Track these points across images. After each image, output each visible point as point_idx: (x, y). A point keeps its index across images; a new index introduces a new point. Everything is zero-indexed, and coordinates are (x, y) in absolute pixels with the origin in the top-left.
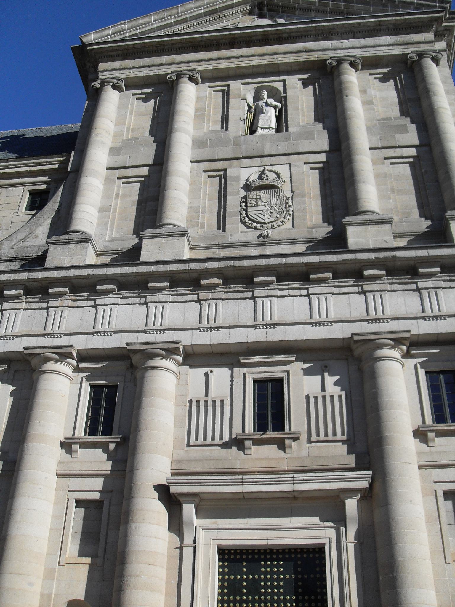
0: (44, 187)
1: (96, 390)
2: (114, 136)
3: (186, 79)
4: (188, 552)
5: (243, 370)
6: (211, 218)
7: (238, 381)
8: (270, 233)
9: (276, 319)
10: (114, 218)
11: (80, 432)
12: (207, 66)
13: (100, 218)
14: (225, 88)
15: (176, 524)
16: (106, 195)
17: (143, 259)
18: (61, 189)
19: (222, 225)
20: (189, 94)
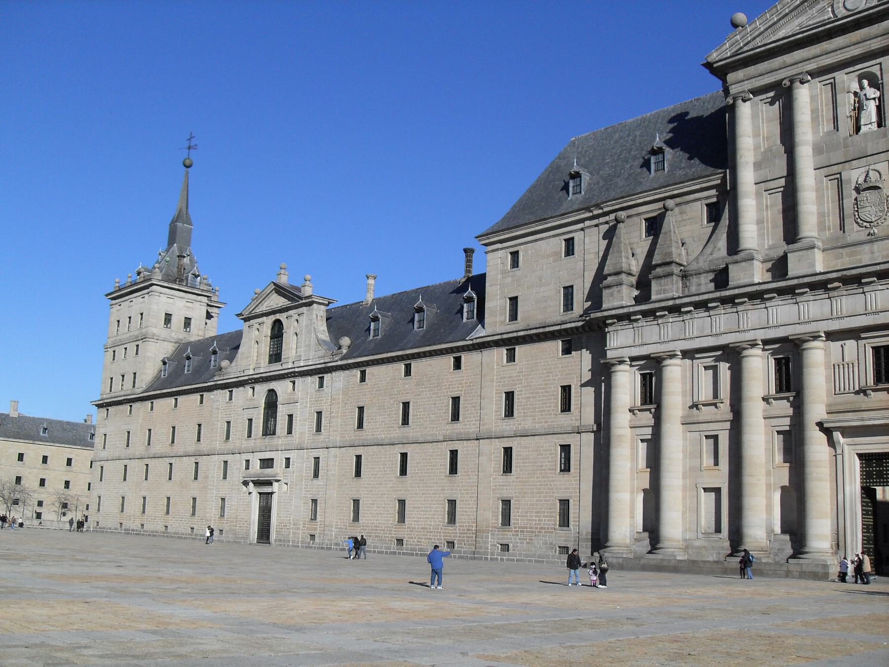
0: (714, 200)
1: (778, 362)
2: (754, 150)
3: (797, 84)
4: (839, 457)
5: (864, 341)
6: (833, 220)
7: (862, 349)
8: (876, 231)
9: (879, 308)
10: (768, 228)
11: (773, 391)
12: (812, 66)
13: (759, 230)
14: (832, 80)
15: (831, 443)
16: (759, 209)
17: (791, 274)
18: (727, 206)
19: (842, 227)
20: (803, 95)
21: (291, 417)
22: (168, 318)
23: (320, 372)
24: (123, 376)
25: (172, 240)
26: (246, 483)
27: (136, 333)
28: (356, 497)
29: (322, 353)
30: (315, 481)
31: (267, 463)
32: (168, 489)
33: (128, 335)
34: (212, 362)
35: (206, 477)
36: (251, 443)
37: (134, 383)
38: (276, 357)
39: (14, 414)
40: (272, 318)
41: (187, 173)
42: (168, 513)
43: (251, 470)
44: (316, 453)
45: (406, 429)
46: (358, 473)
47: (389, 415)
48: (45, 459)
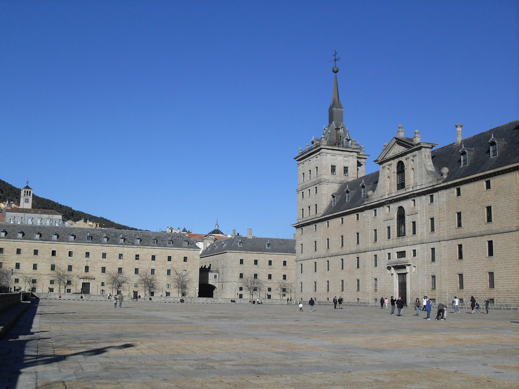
21: (414, 223)
22: (333, 168)
23: (431, 192)
24: (309, 207)
25: (331, 120)
26: (389, 268)
27: (315, 180)
28: (460, 272)
29: (430, 179)
30: (433, 264)
31: (402, 254)
32: (342, 275)
33: (310, 182)
34: (363, 193)
35: (364, 266)
36: (390, 242)
37: (316, 211)
38: (401, 185)
39: (250, 237)
40: (397, 160)
41: (336, 76)
42: (343, 290)
43: (392, 260)
44: (432, 245)
45: (490, 225)
46: (461, 257)
47: (478, 216)
48: (270, 263)
